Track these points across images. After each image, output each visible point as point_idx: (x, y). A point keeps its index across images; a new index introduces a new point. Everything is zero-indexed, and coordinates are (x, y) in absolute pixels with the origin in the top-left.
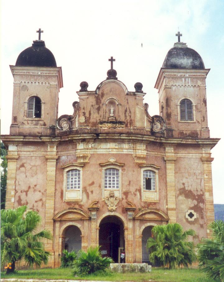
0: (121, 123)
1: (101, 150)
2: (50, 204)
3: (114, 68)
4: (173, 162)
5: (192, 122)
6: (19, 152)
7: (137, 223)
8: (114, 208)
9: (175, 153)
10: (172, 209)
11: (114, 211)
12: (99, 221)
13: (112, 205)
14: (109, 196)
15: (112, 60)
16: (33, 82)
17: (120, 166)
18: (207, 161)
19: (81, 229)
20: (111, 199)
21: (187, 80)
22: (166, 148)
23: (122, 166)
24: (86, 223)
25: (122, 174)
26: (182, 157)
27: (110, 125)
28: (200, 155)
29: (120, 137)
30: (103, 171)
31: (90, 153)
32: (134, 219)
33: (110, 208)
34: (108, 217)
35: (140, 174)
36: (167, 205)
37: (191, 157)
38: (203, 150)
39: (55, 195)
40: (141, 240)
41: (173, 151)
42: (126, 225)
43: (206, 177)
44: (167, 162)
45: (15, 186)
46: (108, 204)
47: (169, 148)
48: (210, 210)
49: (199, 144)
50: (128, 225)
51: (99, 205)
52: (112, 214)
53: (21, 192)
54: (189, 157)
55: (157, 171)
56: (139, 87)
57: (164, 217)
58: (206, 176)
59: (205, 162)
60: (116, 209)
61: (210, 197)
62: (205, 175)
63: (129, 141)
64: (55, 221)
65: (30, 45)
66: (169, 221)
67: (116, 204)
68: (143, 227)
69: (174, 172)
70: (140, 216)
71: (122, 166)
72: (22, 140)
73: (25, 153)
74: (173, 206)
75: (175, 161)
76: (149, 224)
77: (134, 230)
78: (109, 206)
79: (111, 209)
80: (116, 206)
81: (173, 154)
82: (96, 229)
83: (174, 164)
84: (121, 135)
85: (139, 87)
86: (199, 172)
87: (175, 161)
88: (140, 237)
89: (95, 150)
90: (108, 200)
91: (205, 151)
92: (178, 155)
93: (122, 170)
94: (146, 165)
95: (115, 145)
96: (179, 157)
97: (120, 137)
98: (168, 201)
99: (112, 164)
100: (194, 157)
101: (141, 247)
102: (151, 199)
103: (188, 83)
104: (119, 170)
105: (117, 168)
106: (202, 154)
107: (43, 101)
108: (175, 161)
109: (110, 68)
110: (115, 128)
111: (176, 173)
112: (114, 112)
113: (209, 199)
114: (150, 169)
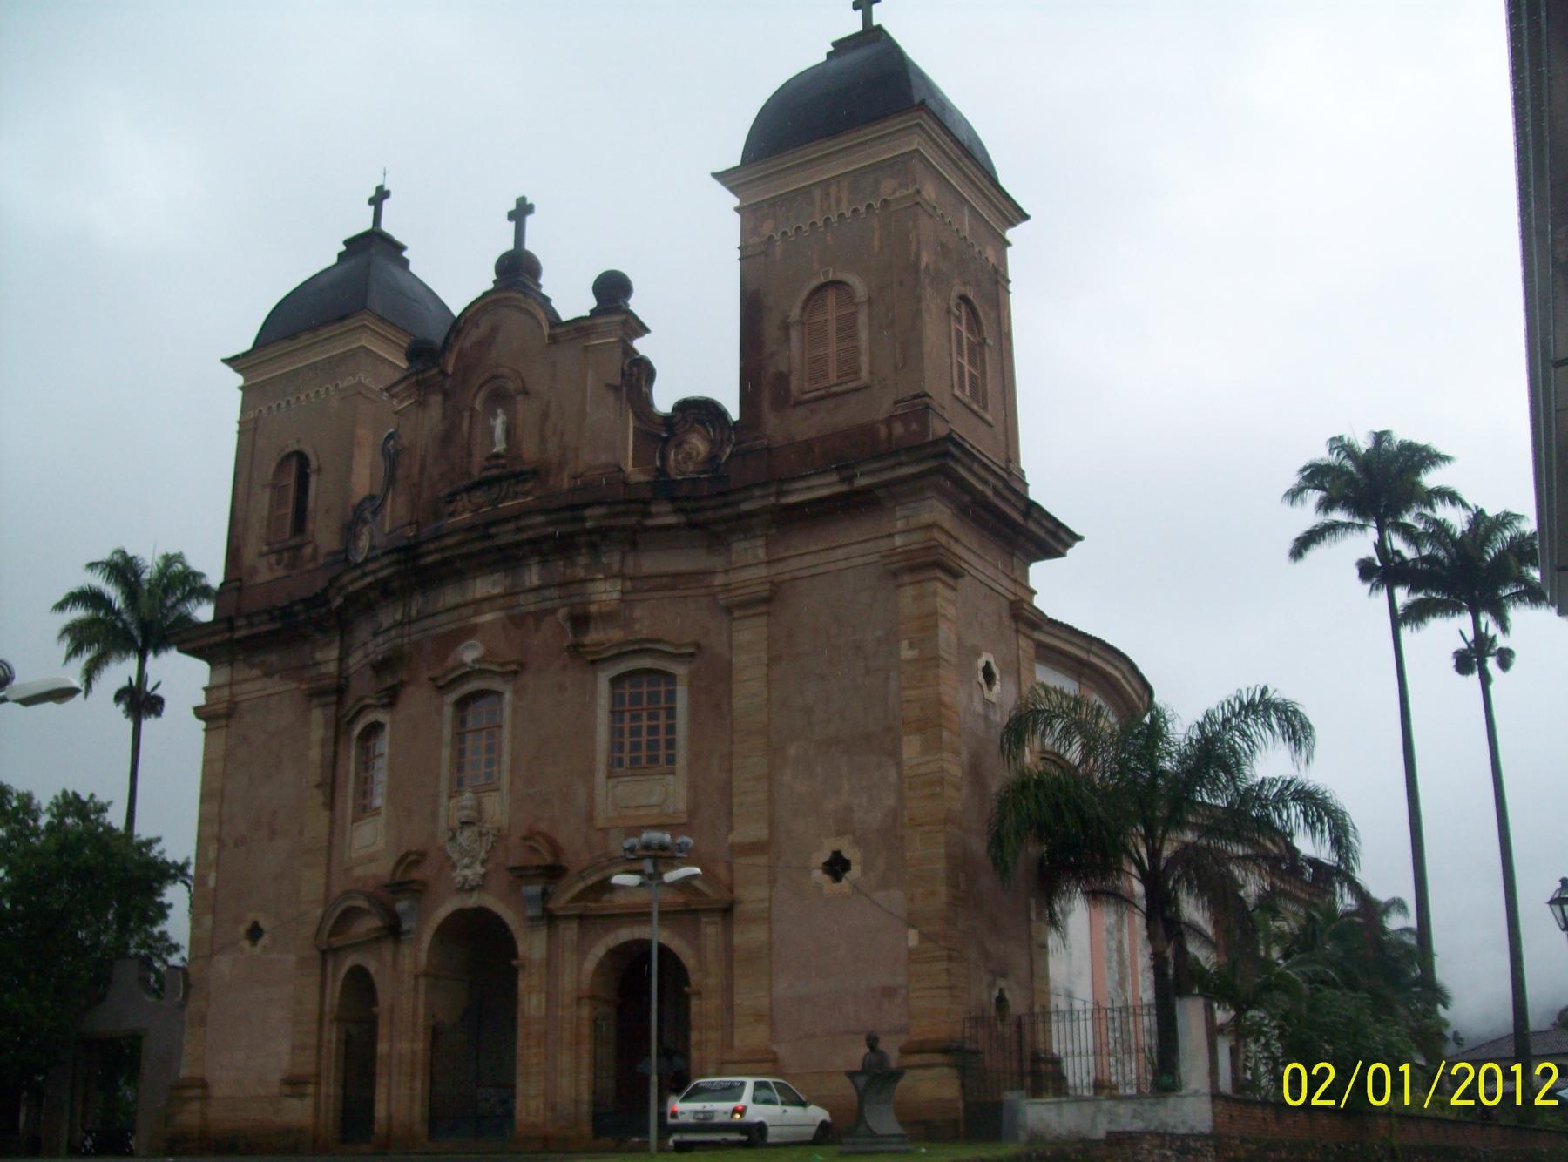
0: (519, 477)
1: (442, 618)
2: (312, 883)
3: (530, 245)
4: (762, 609)
5: (852, 385)
6: (236, 689)
7: (570, 932)
8: (473, 873)
9: (768, 562)
10: (753, 848)
11: (473, 889)
12: (427, 938)
13: (466, 861)
14: (457, 824)
15: (521, 212)
16: (293, 401)
17: (503, 675)
18: (912, 569)
19: (377, 980)
20: (465, 837)
21: (833, 190)
22: (736, 546)
23: (514, 672)
24: (387, 951)
25: (515, 711)
26: (797, 574)
27: (479, 496)
28: (885, 544)
29: (487, 544)
30: (448, 711)
31: (415, 637)
32: (550, 919)
33: (459, 875)
34: (459, 915)
35: (594, 694)
36: (731, 829)
37: (842, 564)
38: (898, 514)
39: (330, 844)
40: (585, 1012)
41: (761, 553)
42: (522, 948)
43: (907, 653)
44: (737, 614)
45: (221, 824)
46: (455, 856)
47: (746, 544)
48: (927, 828)
49: (867, 490)
50: (532, 946)
51: (424, 872)
52: (472, 901)
53: (236, 845)
54: (831, 567)
55: (681, 670)
56: (612, 288)
57: (706, 895)
58: (911, 646)
59: (907, 578)
60: (484, 876)
61: (926, 759)
62: (905, 643)
63: (539, 548)
64: (323, 953)
65: (324, 255)
66: (738, 909)
67: (483, 855)
68: (599, 951)
69: (765, 661)
70: (575, 899)
71: (516, 673)
72: (227, 635)
73: (248, 686)
74: (750, 830)
75: (770, 599)
76: (625, 934)
77: (550, 964)
78: (460, 866)
79: (467, 880)
80: (483, 863)
81: (763, 571)
82: (416, 977)
83: (763, 621)
84: (493, 530)
85: (612, 288)
86: (879, 633)
87: (770, 599)
88: (579, 999)
89: (427, 623)
90: (453, 838)
91: (907, 517)
92: (780, 567)
93: (516, 692)
94: (615, 651)
95: (494, 584)
96: (787, 576)
97: (487, 544)
98: (736, 810)
99: (481, 673)
100: (860, 561)
101: (585, 1048)
102: (642, 812)
103: (839, 201)
104: (499, 694)
105: (495, 684)
106: (891, 535)
107: (314, 464)
108: (768, 600)
109: (509, 245)
110: (494, 503)
111: (773, 660)
112: (509, 433)
113: (923, 769)
114: (647, 663)
